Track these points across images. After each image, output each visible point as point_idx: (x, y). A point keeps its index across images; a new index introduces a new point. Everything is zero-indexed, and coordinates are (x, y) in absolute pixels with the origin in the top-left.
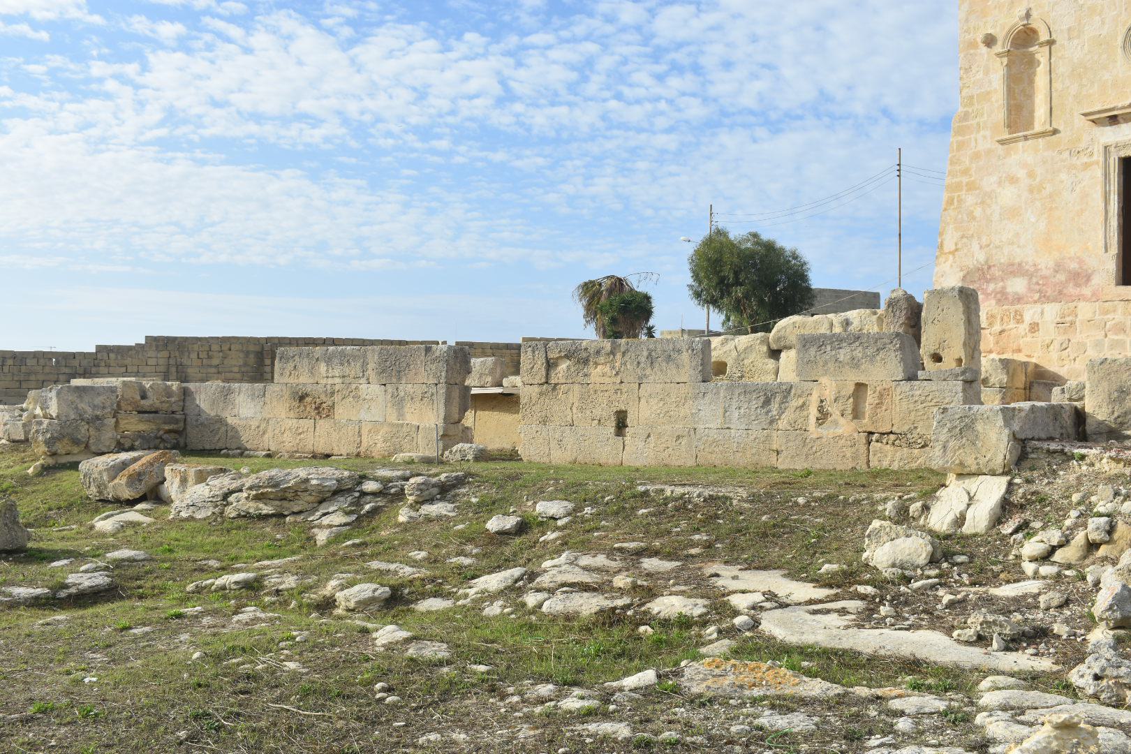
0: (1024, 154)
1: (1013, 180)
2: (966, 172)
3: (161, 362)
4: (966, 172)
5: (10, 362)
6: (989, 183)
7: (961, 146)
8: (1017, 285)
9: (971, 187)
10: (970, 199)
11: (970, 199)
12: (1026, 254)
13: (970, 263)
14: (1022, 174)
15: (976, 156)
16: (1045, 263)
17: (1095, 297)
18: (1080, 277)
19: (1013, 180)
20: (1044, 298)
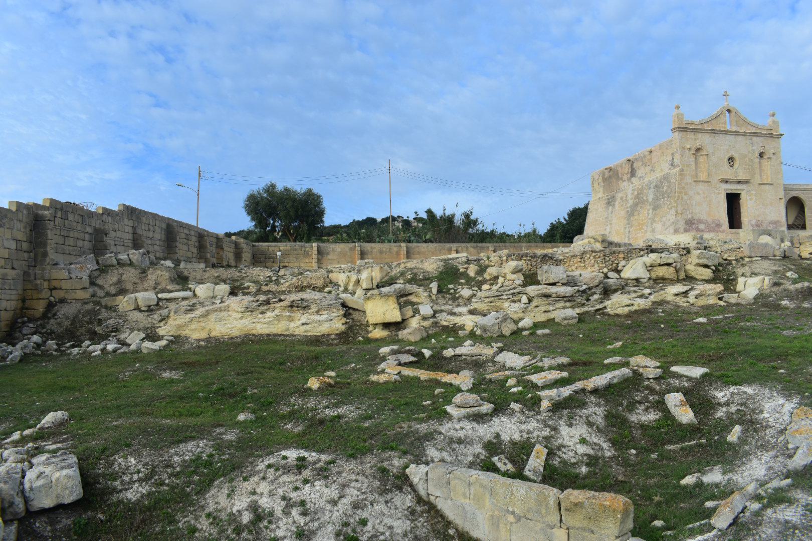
0: (701, 187)
1: (698, 194)
2: (683, 188)
3: (130, 230)
4: (683, 188)
5: (59, 214)
6: (691, 193)
7: (681, 180)
8: (702, 226)
9: (686, 193)
10: (685, 197)
11: (685, 197)
12: (704, 217)
13: (686, 218)
14: (701, 192)
15: (687, 184)
16: (710, 220)
17: (724, 231)
18: (719, 225)
19: (698, 194)
20: (710, 231)
